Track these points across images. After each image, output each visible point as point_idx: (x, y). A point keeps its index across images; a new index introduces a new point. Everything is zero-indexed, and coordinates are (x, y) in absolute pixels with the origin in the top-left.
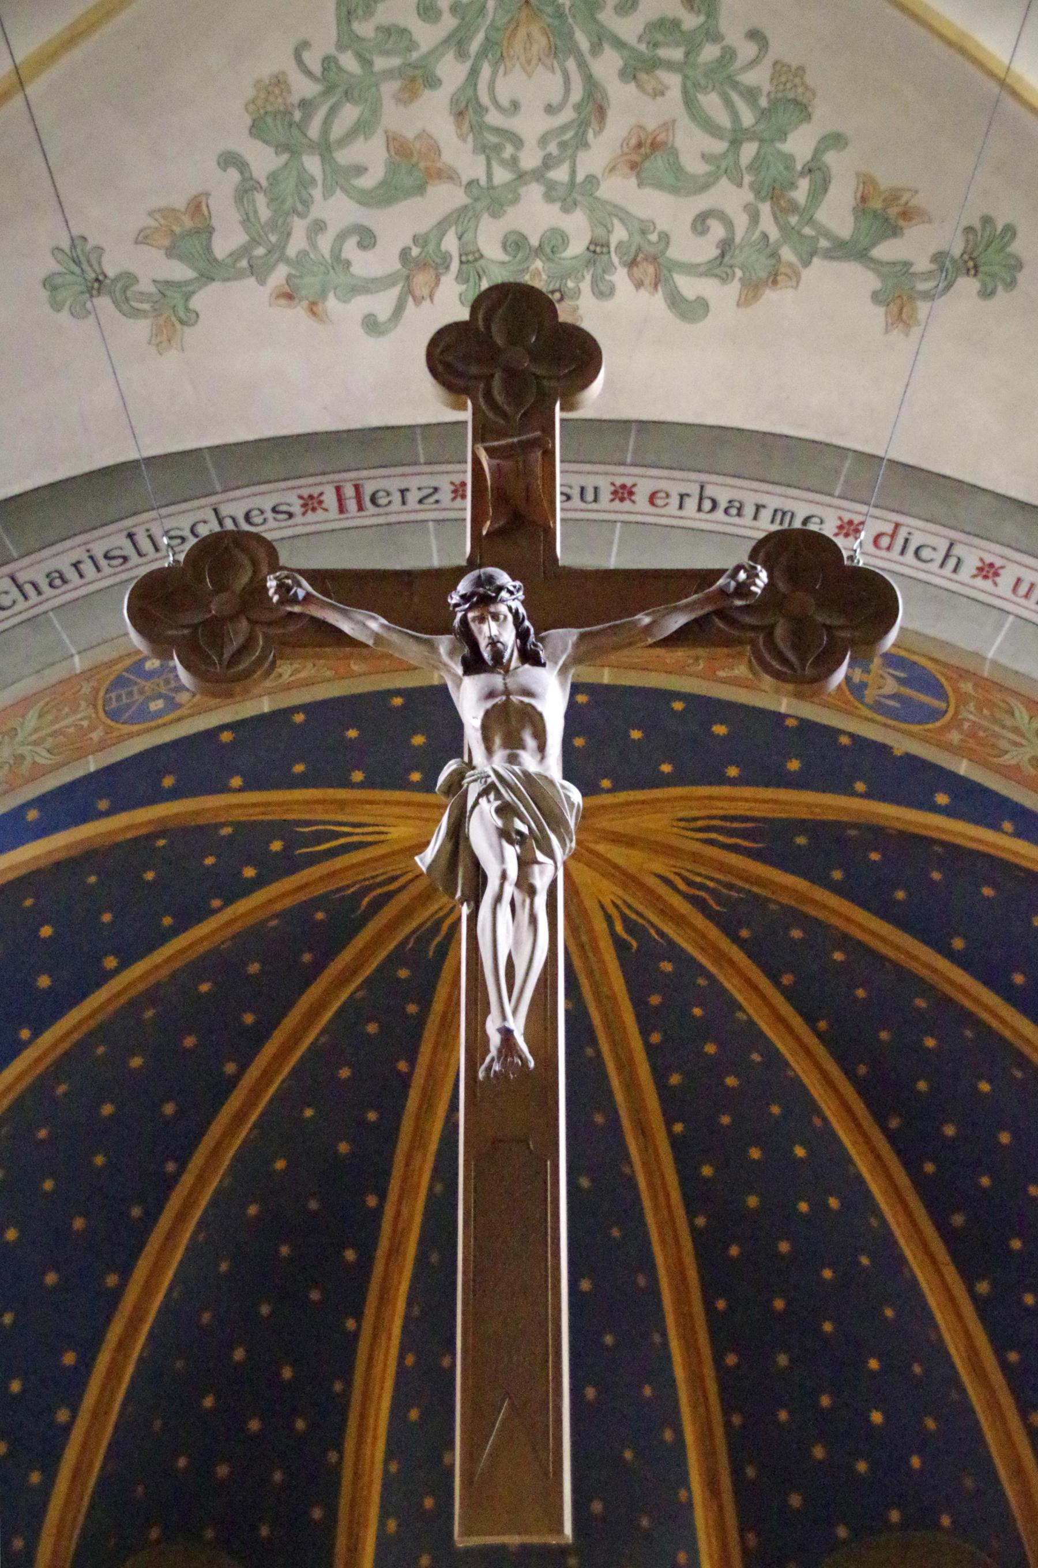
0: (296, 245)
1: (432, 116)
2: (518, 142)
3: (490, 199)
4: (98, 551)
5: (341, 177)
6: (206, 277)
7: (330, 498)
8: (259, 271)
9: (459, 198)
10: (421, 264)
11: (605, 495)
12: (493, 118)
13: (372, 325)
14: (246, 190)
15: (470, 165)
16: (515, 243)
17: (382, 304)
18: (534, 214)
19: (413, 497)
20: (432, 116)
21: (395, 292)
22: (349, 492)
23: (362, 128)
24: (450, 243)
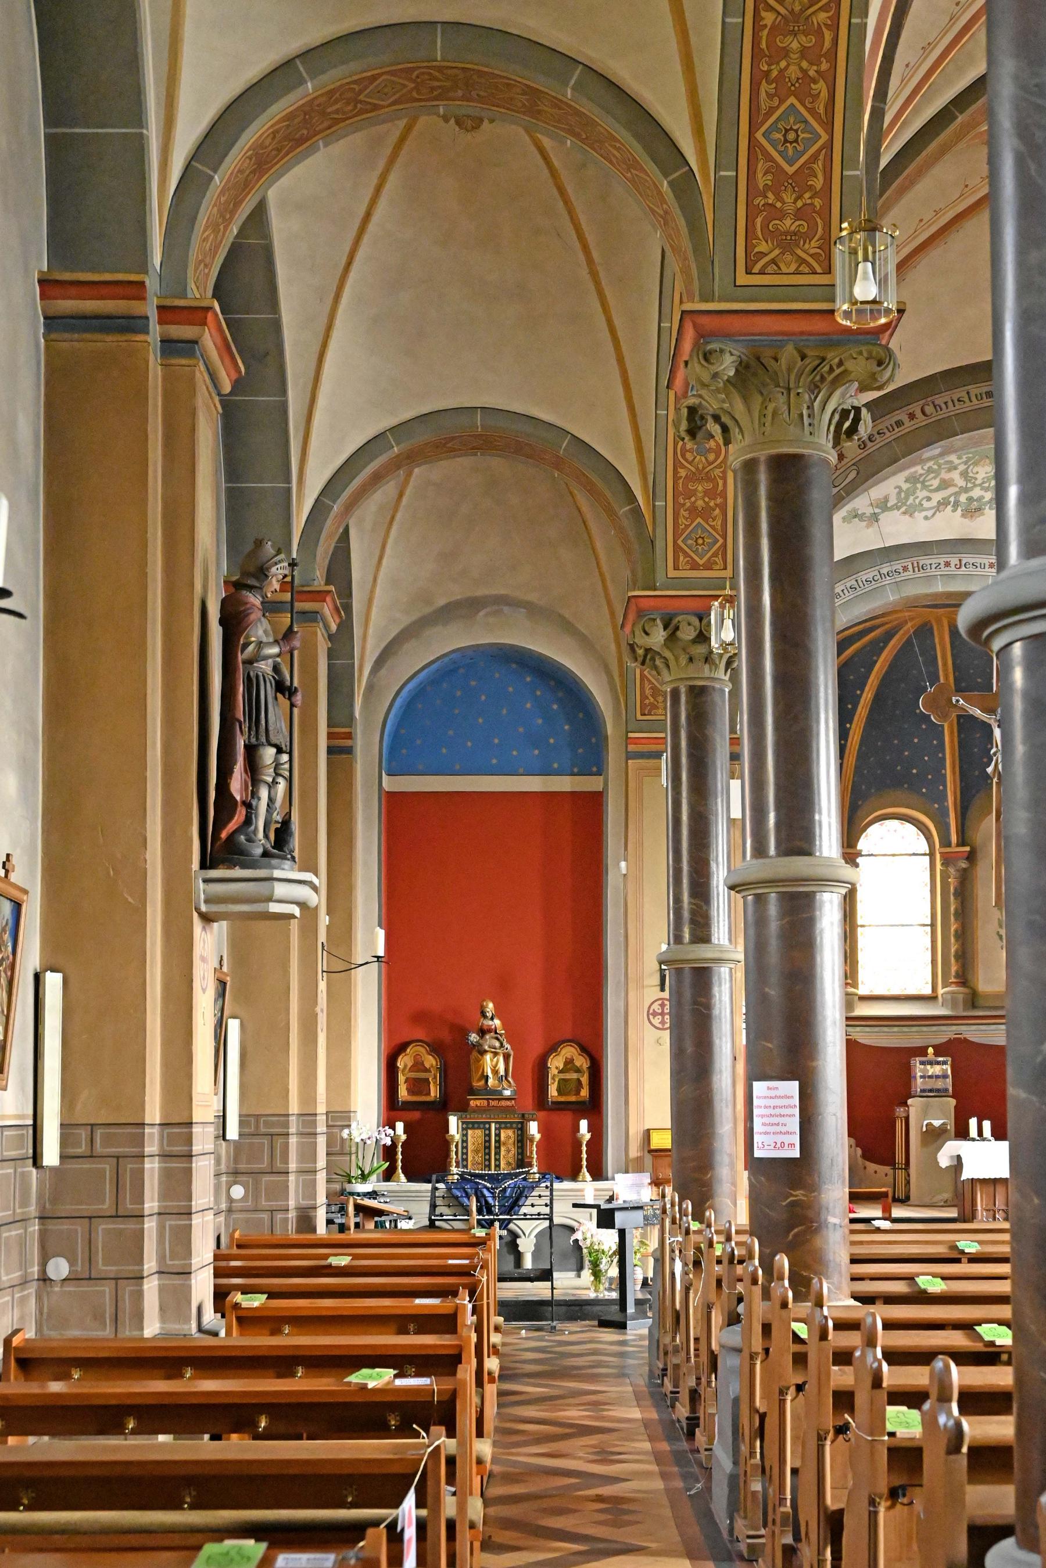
0: (910, 501)
1: (955, 475)
2: (976, 479)
3: (966, 490)
4: (848, 586)
5: (925, 487)
6: (883, 512)
7: (910, 567)
8: (898, 509)
9: (957, 489)
10: (943, 504)
11: (987, 566)
12: (971, 475)
13: (926, 518)
14: (899, 493)
15: (963, 484)
16: (970, 499)
17: (929, 513)
18: (976, 493)
19: (934, 566)
20: (955, 475)
21: (933, 511)
22: (915, 565)
23: (935, 478)
24: (952, 499)
